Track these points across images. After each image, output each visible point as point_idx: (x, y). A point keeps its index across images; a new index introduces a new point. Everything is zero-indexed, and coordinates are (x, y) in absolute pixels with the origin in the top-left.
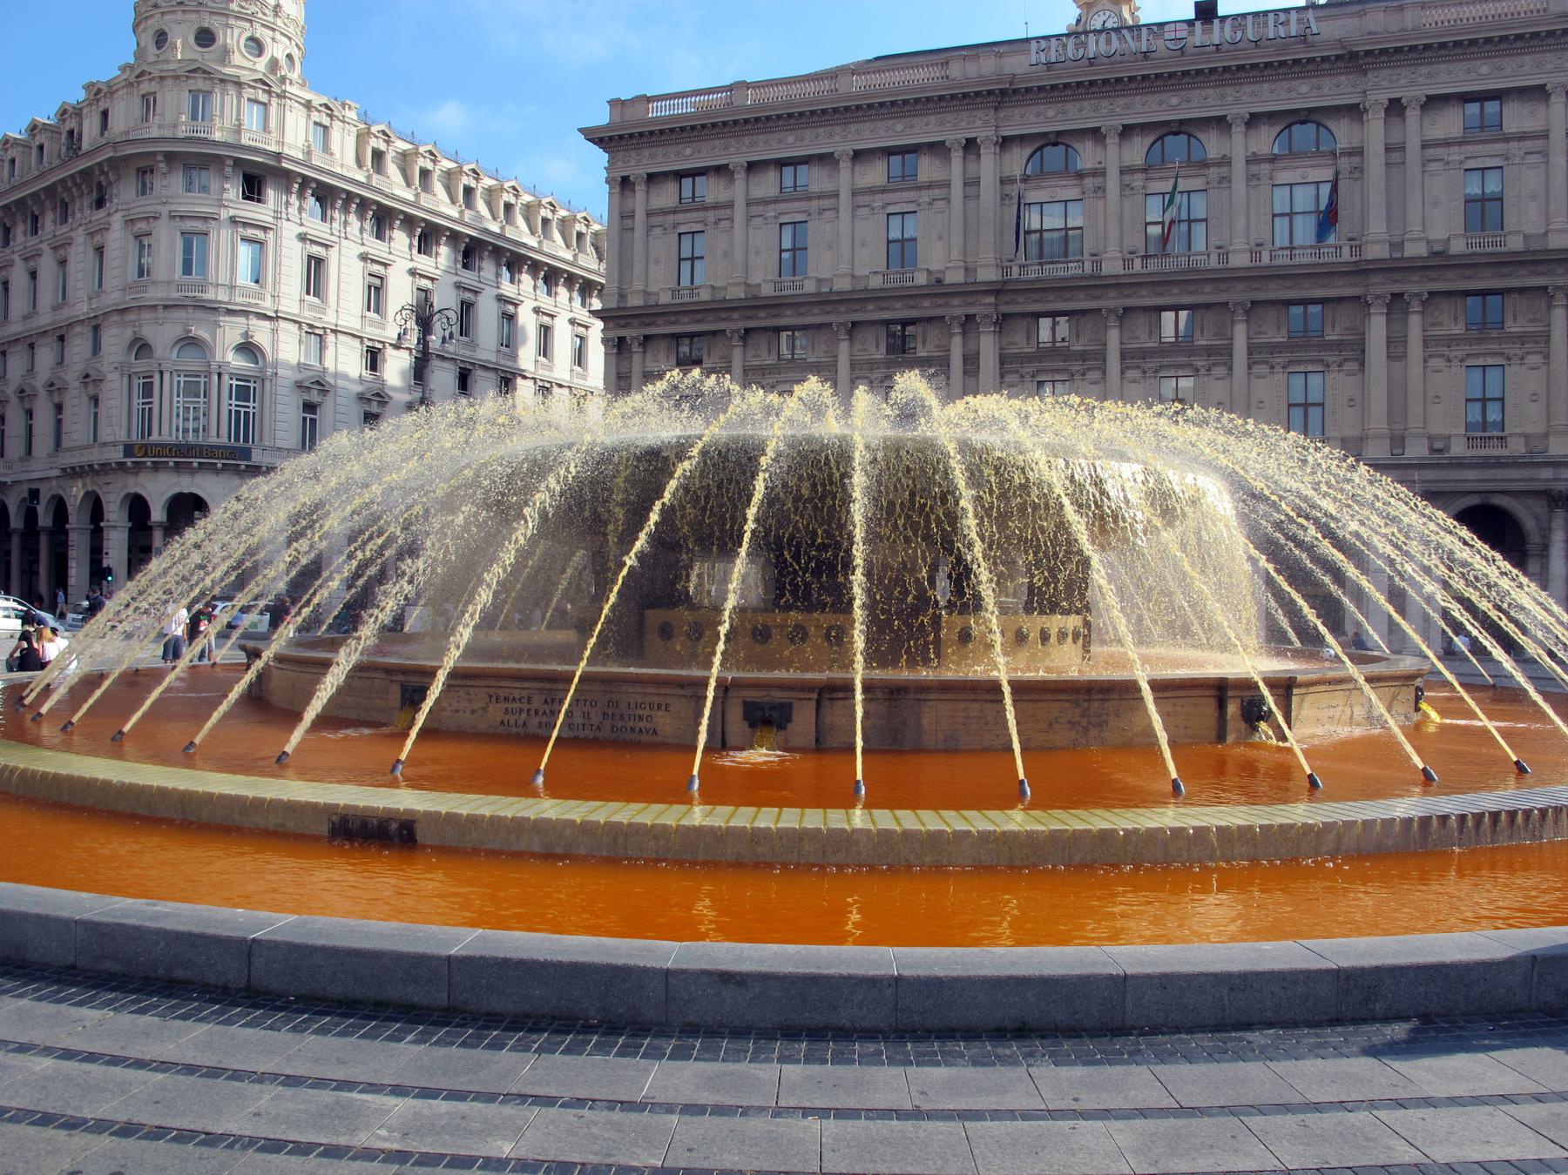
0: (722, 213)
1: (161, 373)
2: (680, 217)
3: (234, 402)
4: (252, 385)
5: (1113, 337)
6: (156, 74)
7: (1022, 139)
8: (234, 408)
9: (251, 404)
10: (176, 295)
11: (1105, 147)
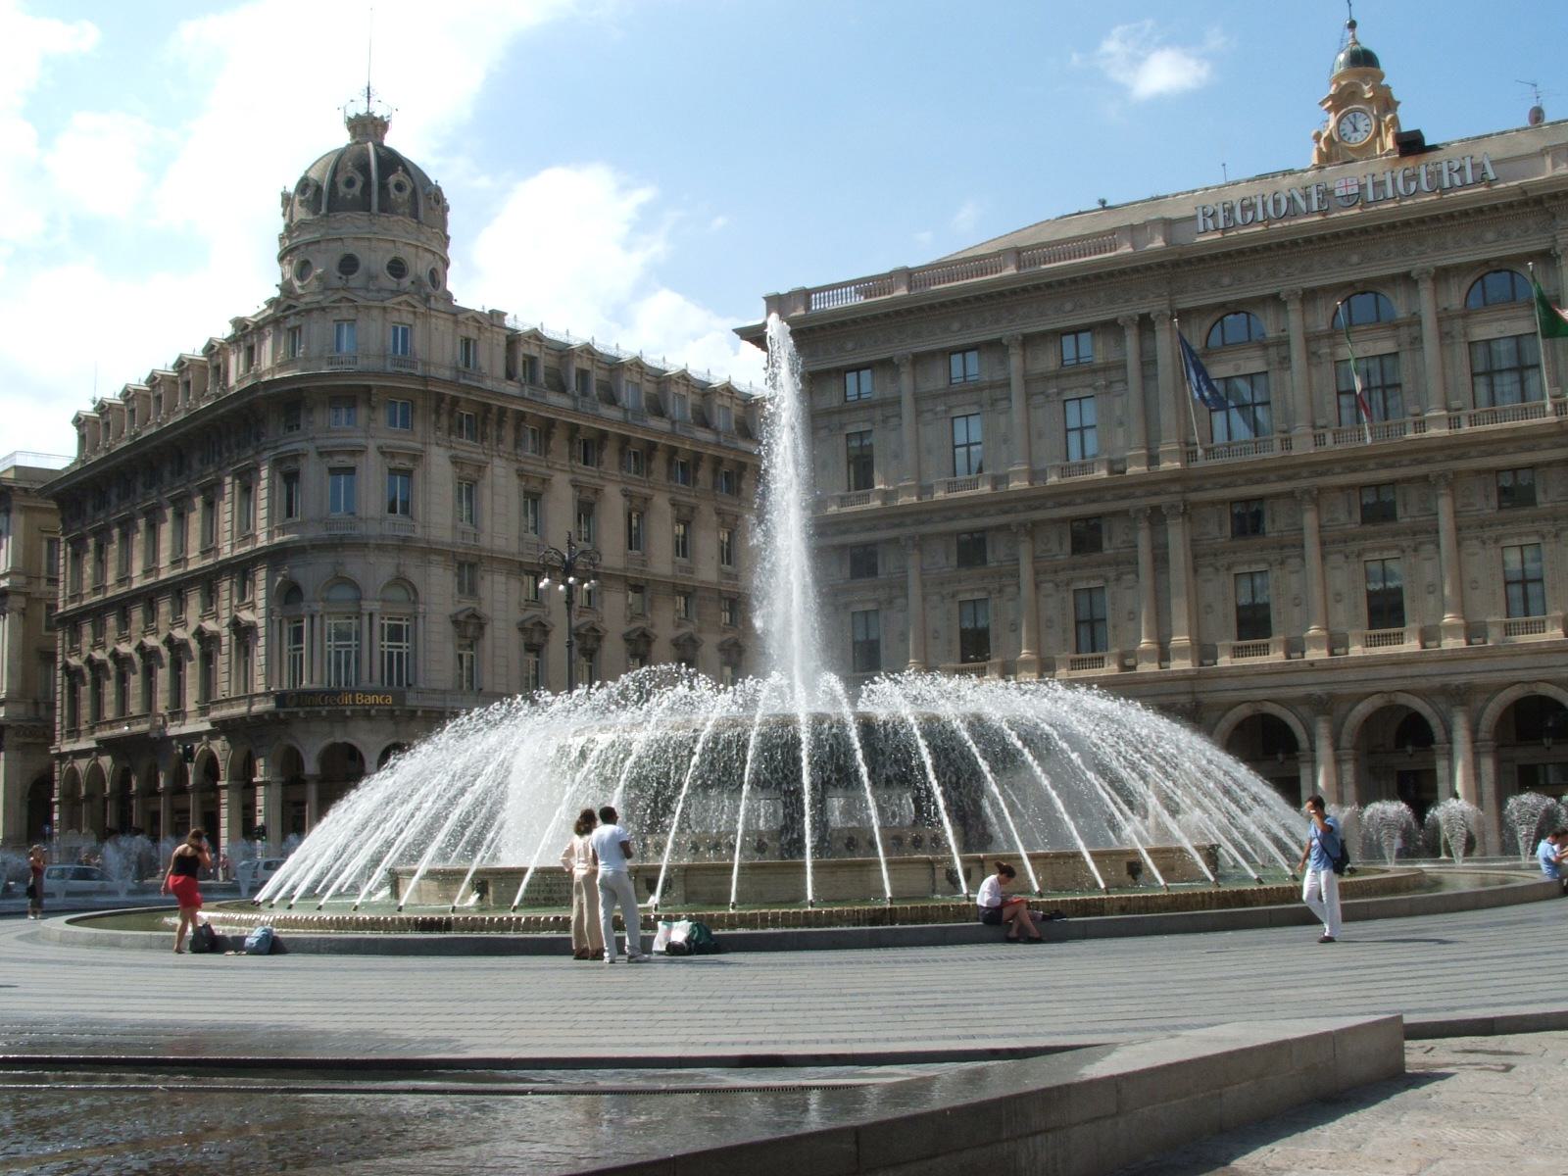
1: (312, 617)
3: (386, 643)
4: (404, 623)
5: (1310, 520)
6: (302, 307)
8: (386, 650)
9: (404, 644)
10: (324, 534)
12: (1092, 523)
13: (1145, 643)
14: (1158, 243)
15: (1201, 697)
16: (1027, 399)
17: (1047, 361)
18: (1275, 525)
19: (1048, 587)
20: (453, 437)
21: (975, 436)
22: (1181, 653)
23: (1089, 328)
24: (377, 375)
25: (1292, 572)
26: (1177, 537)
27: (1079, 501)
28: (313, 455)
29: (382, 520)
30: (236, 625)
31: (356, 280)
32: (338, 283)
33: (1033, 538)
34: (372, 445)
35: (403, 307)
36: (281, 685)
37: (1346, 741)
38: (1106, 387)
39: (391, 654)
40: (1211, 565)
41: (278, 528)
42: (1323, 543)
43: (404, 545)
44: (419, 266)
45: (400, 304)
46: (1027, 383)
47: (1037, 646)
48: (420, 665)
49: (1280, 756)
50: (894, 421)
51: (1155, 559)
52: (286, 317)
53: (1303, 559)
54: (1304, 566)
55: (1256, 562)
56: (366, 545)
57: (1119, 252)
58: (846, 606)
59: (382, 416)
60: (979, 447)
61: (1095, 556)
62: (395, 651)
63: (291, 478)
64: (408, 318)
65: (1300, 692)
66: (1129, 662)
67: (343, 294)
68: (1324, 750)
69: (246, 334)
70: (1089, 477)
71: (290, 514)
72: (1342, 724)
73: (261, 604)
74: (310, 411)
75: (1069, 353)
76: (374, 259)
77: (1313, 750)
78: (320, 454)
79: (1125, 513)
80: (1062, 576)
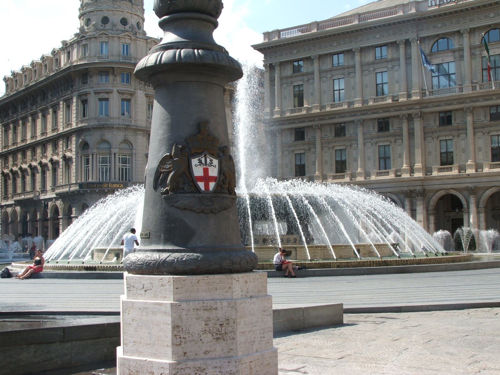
0: (310, 77)
1: (93, 155)
2: (293, 79)
3: (121, 165)
4: (128, 157)
5: (469, 119)
6: (88, 37)
7: (428, 38)
8: (121, 167)
9: (128, 165)
11: (463, 38)
12: (386, 120)
13: (405, 166)
14: (413, 11)
15: (426, 187)
16: (362, 72)
17: (370, 58)
18: (456, 122)
19: (369, 145)
20: (146, 87)
21: (342, 87)
22: (418, 170)
23: (386, 45)
24: (116, 63)
25: (461, 140)
26: (418, 125)
27: (380, 111)
28: (92, 94)
29: (119, 118)
30: (64, 157)
31: (108, 26)
32: (102, 28)
33: (321, 131)
34: (115, 90)
35: (127, 37)
36: (81, 180)
37: (482, 205)
38: (392, 68)
39: (122, 169)
40: (431, 137)
41: (80, 121)
42: (474, 128)
43: (127, 128)
44: (133, 21)
45: (125, 35)
46: (361, 66)
47: (364, 167)
48: (134, 174)
49: (457, 210)
50: (311, 81)
51: (409, 134)
52: (82, 41)
53: (467, 134)
54: (466, 137)
55: (448, 136)
56: (113, 128)
57: (398, 15)
58: (293, 151)
59: (119, 79)
60: (343, 91)
61: (387, 133)
62: (124, 168)
63: (85, 102)
64: (128, 41)
65: (464, 186)
66: (399, 174)
67: (103, 32)
68: (473, 208)
69: (67, 47)
70: (384, 102)
71: (84, 116)
72: (480, 198)
73: (74, 150)
74: (91, 77)
75: (378, 54)
76: (115, 18)
77: (468, 208)
78: (95, 93)
79: (398, 116)
80: (374, 141)
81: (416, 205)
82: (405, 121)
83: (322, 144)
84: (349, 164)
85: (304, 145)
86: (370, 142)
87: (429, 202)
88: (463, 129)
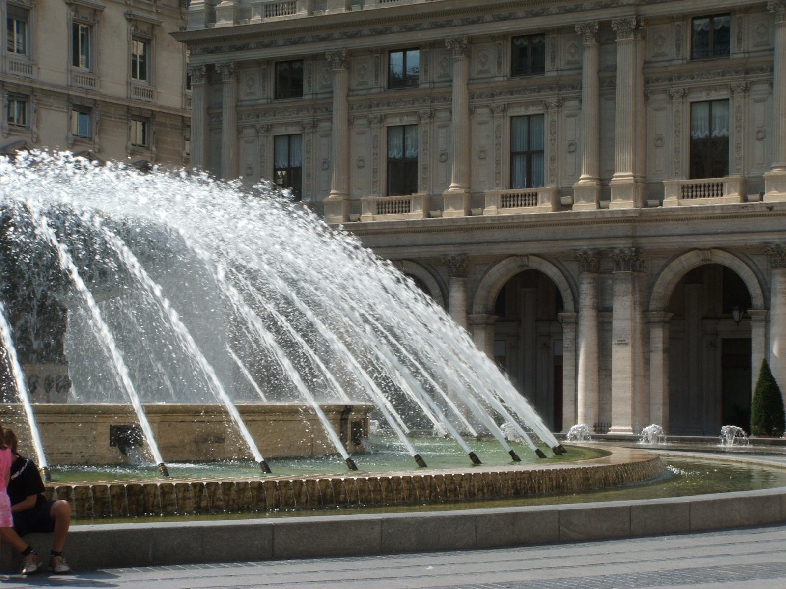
13: (584, 179)
15: (643, 241)
18: (740, 48)
22: (623, 191)
25: (756, 101)
26: (627, 57)
27: (520, 14)
40: (665, 91)
47: (467, 179)
53: (772, 85)
54: (771, 93)
55: (715, 88)
58: (269, 128)
61: (536, 79)
65: (755, 240)
66: (566, 200)
80: (500, 101)
81: (612, 296)
82: (591, 43)
83: (350, 107)
84: (425, 168)
85: (299, 110)
86: (487, 106)
87: (650, 287)
88: (762, 70)
